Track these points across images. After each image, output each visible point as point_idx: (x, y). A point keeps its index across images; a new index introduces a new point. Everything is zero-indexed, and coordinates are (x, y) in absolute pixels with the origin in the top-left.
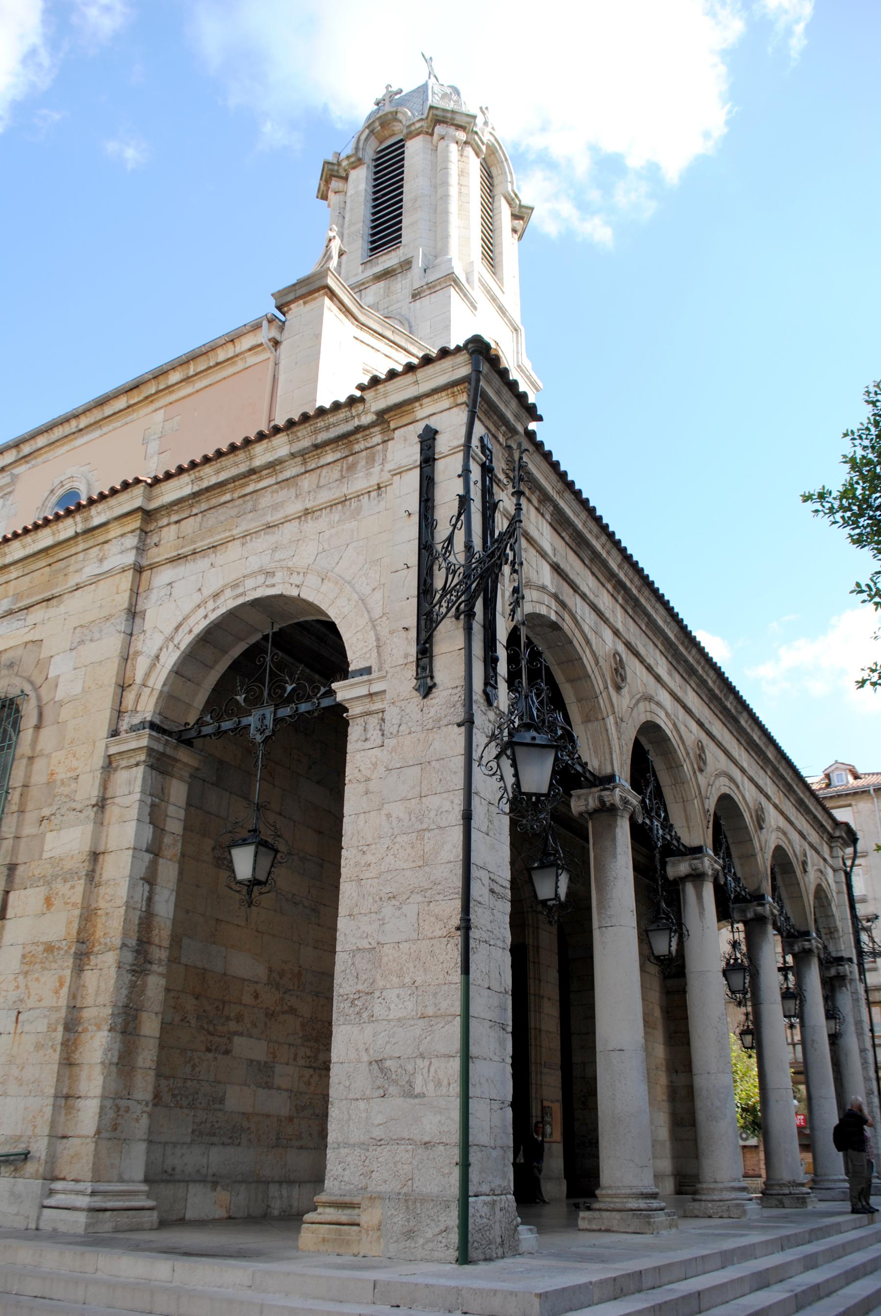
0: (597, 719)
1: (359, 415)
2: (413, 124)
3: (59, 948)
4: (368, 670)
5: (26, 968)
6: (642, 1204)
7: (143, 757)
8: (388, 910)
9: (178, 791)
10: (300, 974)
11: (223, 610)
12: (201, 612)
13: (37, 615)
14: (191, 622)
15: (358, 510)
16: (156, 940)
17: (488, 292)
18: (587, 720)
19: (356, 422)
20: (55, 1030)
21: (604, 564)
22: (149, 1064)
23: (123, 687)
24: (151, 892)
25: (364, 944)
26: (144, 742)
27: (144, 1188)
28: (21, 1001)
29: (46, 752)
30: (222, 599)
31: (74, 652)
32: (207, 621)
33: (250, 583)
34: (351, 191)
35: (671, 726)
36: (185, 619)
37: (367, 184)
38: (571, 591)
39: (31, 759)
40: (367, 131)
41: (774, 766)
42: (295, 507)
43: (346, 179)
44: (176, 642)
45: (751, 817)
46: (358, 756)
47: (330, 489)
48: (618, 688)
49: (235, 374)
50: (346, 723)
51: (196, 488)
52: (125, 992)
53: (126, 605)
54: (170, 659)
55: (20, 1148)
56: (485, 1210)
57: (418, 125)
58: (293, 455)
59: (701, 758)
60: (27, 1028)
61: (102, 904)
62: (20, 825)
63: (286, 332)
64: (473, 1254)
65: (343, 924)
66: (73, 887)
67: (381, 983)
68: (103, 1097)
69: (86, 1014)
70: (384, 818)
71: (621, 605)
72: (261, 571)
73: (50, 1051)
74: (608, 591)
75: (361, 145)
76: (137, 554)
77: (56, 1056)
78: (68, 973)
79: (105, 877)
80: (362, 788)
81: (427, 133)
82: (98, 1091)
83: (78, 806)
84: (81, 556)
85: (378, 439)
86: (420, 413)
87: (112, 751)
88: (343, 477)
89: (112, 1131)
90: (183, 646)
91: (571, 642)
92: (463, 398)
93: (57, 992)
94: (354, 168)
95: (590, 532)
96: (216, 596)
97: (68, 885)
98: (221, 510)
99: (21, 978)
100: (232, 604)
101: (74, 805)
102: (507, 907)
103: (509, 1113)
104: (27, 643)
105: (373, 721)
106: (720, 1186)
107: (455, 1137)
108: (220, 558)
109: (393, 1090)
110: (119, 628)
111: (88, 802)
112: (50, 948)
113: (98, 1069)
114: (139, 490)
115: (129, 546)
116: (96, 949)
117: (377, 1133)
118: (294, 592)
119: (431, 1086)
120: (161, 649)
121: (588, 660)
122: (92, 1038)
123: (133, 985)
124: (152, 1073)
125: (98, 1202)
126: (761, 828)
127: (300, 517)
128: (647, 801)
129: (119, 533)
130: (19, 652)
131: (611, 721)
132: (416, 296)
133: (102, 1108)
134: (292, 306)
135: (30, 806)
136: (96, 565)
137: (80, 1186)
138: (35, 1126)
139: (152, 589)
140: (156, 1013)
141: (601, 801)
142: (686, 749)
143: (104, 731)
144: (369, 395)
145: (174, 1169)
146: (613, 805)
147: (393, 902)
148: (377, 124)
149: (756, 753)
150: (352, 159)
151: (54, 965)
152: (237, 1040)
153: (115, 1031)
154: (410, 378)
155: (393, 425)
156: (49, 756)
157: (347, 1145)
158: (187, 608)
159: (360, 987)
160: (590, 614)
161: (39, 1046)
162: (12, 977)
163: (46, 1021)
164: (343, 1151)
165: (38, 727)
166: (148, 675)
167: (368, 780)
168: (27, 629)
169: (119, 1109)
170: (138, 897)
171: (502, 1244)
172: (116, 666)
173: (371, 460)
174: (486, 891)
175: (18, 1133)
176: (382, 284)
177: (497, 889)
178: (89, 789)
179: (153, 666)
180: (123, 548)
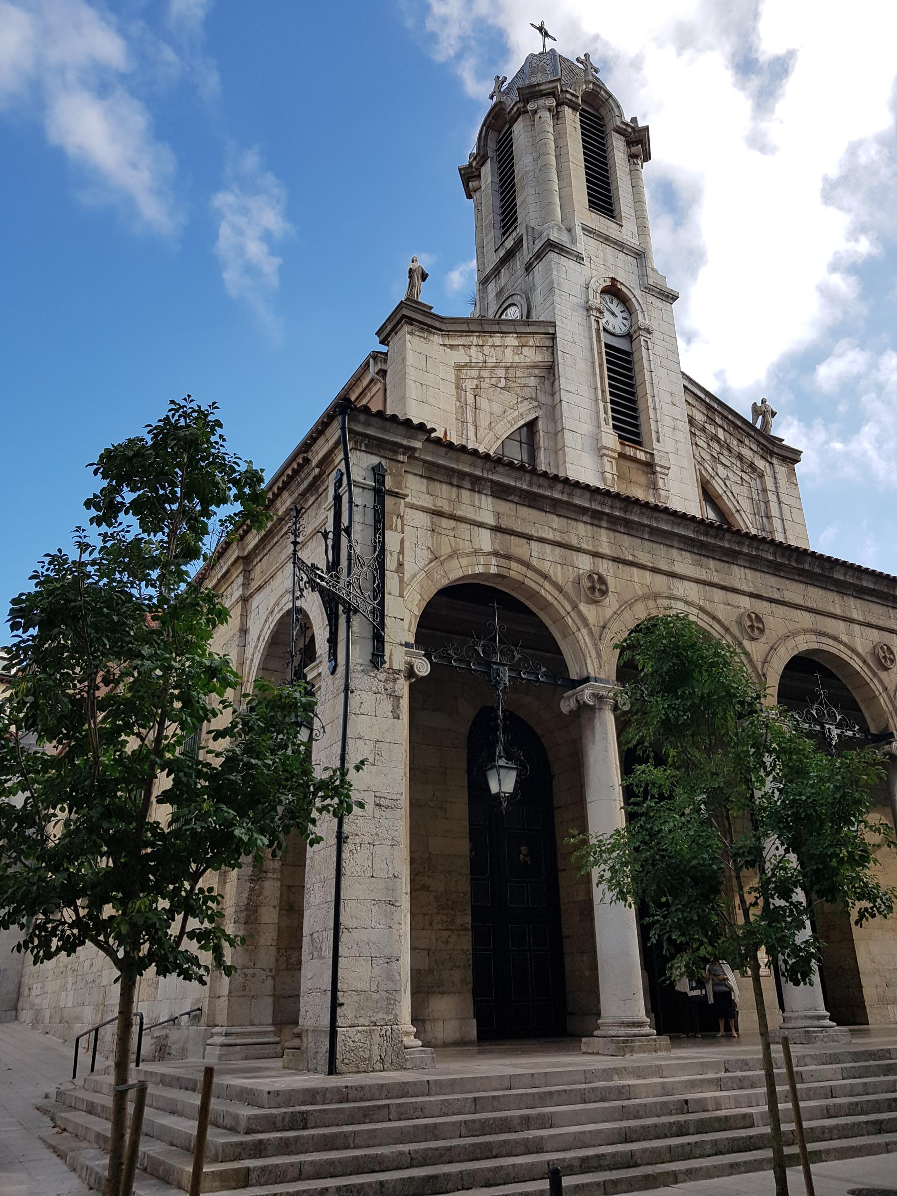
10: (430, 859)
18: (564, 637)
22: (270, 942)
27: (271, 1028)
45: (865, 662)
52: (246, 895)
71: (607, 528)
74: (585, 523)
95: (540, 486)
96: (272, 612)
114: (234, 545)
123: (252, 890)
124: (274, 949)
140: (274, 907)
149: (877, 597)
153: (239, 923)
179: (251, 666)
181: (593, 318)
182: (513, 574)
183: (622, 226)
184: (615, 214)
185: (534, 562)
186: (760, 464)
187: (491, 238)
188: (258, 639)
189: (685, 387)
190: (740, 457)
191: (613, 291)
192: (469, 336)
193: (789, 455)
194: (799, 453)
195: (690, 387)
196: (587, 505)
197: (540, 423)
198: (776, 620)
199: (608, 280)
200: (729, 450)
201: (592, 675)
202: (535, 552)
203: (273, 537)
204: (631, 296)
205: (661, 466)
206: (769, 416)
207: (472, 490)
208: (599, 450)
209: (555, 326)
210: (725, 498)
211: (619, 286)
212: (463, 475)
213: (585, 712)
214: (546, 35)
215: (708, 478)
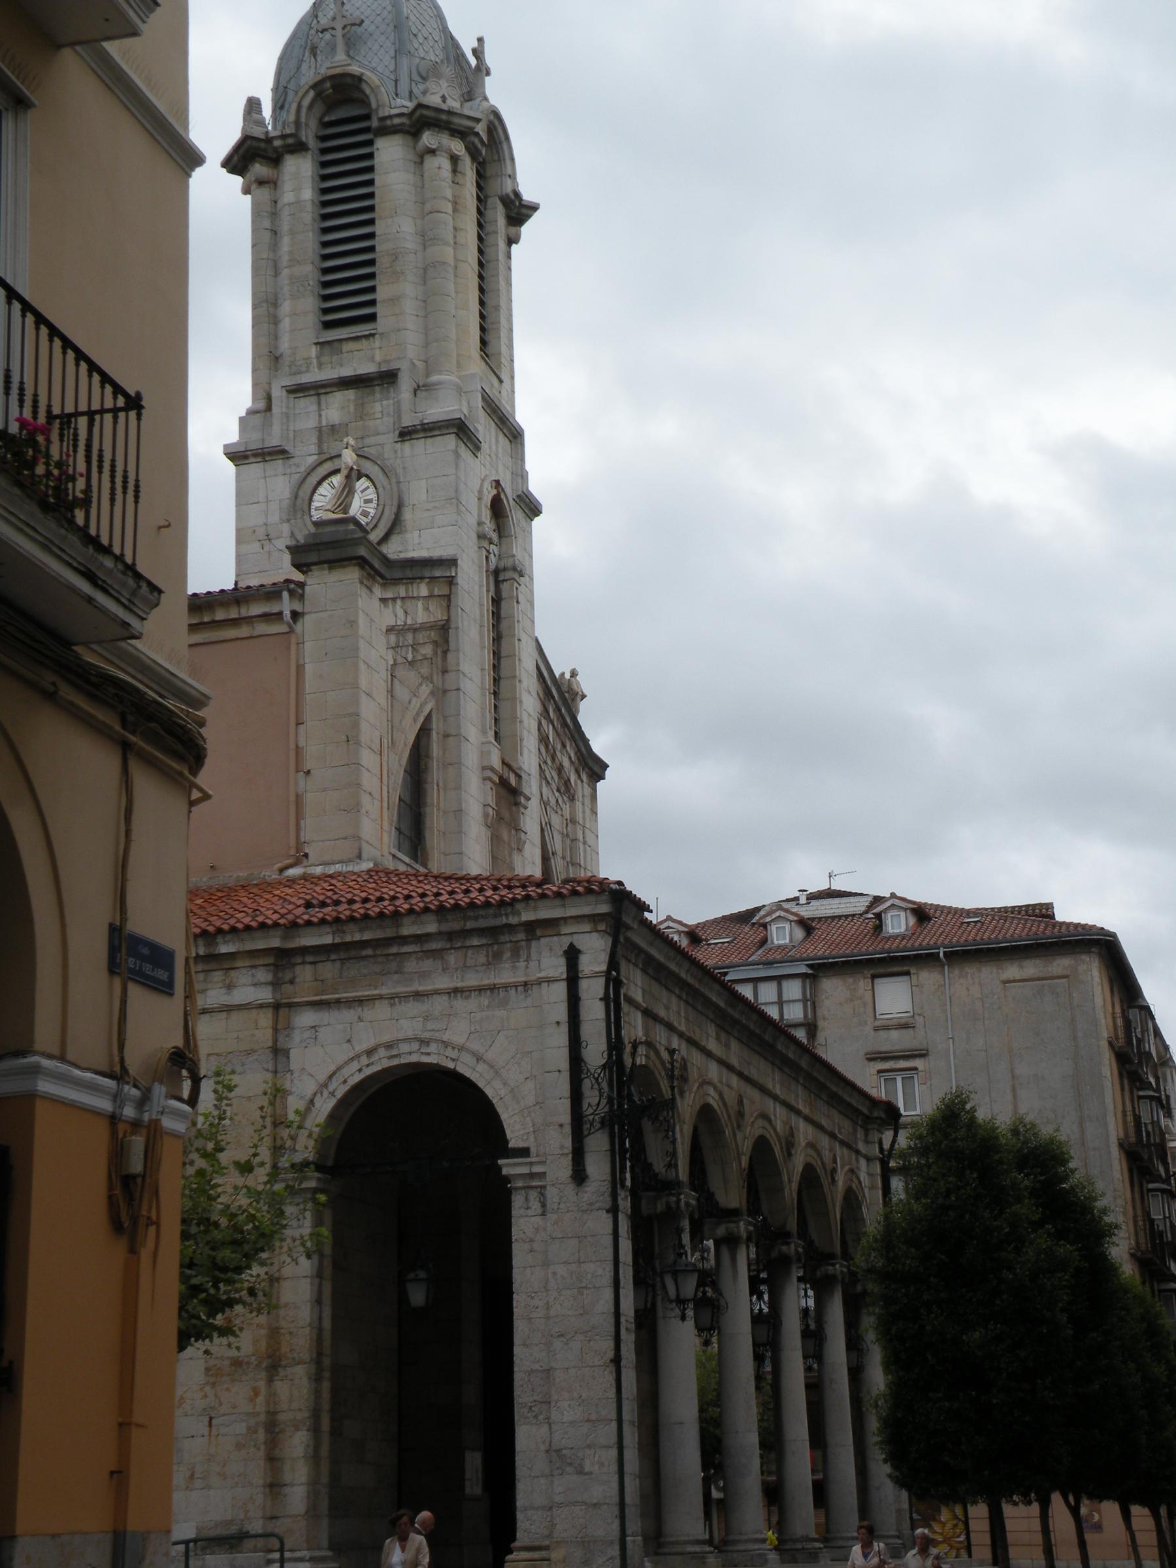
2: (391, 117)
3: (248, 1363)
4: (524, 1152)
5: (212, 1380)
6: (697, 1548)
8: (558, 1344)
12: (355, 1066)
14: (346, 1072)
19: (504, 920)
20: (256, 1432)
25: (537, 1367)
27: (330, 1553)
28: (212, 1408)
30: (375, 1057)
33: (404, 1047)
35: (717, 1097)
36: (339, 1069)
44: (331, 1089)
46: (522, 1221)
51: (338, 940)
53: (270, 1044)
54: (325, 1106)
58: (440, 933)
61: (283, 1324)
63: (306, 602)
65: (518, 1350)
67: (555, 1397)
69: (281, 1417)
72: (416, 1039)
73: (252, 1449)
75: (303, 120)
76: (274, 991)
77: (261, 1453)
78: (262, 1384)
79: (283, 1300)
80: (527, 1246)
81: (408, 133)
82: (304, 1479)
86: (565, 930)
93: (251, 1400)
96: (370, 1052)
99: (208, 1389)
100: (386, 1064)
105: (533, 1195)
106: (745, 1537)
107: (616, 1499)
108: (368, 1013)
109: (568, 1469)
110: (266, 1066)
115: (263, 980)
116: (283, 1363)
117: (558, 1499)
118: (451, 1065)
119: (596, 1467)
120: (315, 1094)
129: (247, 964)
134: (313, 567)
136: (223, 991)
137: (298, 1554)
139: (293, 1028)
148: (328, 85)
150: (290, 141)
154: (558, 902)
157: (532, 1508)
159: (535, 1398)
161: (239, 1446)
163: (244, 1424)
164: (530, 1513)
173: (516, 954)
175: (229, 1518)
176: (351, 394)
180: (255, 981)
183: (501, 381)
186: (573, 778)
188: (331, 1077)
193: (596, 768)
208: (484, 768)
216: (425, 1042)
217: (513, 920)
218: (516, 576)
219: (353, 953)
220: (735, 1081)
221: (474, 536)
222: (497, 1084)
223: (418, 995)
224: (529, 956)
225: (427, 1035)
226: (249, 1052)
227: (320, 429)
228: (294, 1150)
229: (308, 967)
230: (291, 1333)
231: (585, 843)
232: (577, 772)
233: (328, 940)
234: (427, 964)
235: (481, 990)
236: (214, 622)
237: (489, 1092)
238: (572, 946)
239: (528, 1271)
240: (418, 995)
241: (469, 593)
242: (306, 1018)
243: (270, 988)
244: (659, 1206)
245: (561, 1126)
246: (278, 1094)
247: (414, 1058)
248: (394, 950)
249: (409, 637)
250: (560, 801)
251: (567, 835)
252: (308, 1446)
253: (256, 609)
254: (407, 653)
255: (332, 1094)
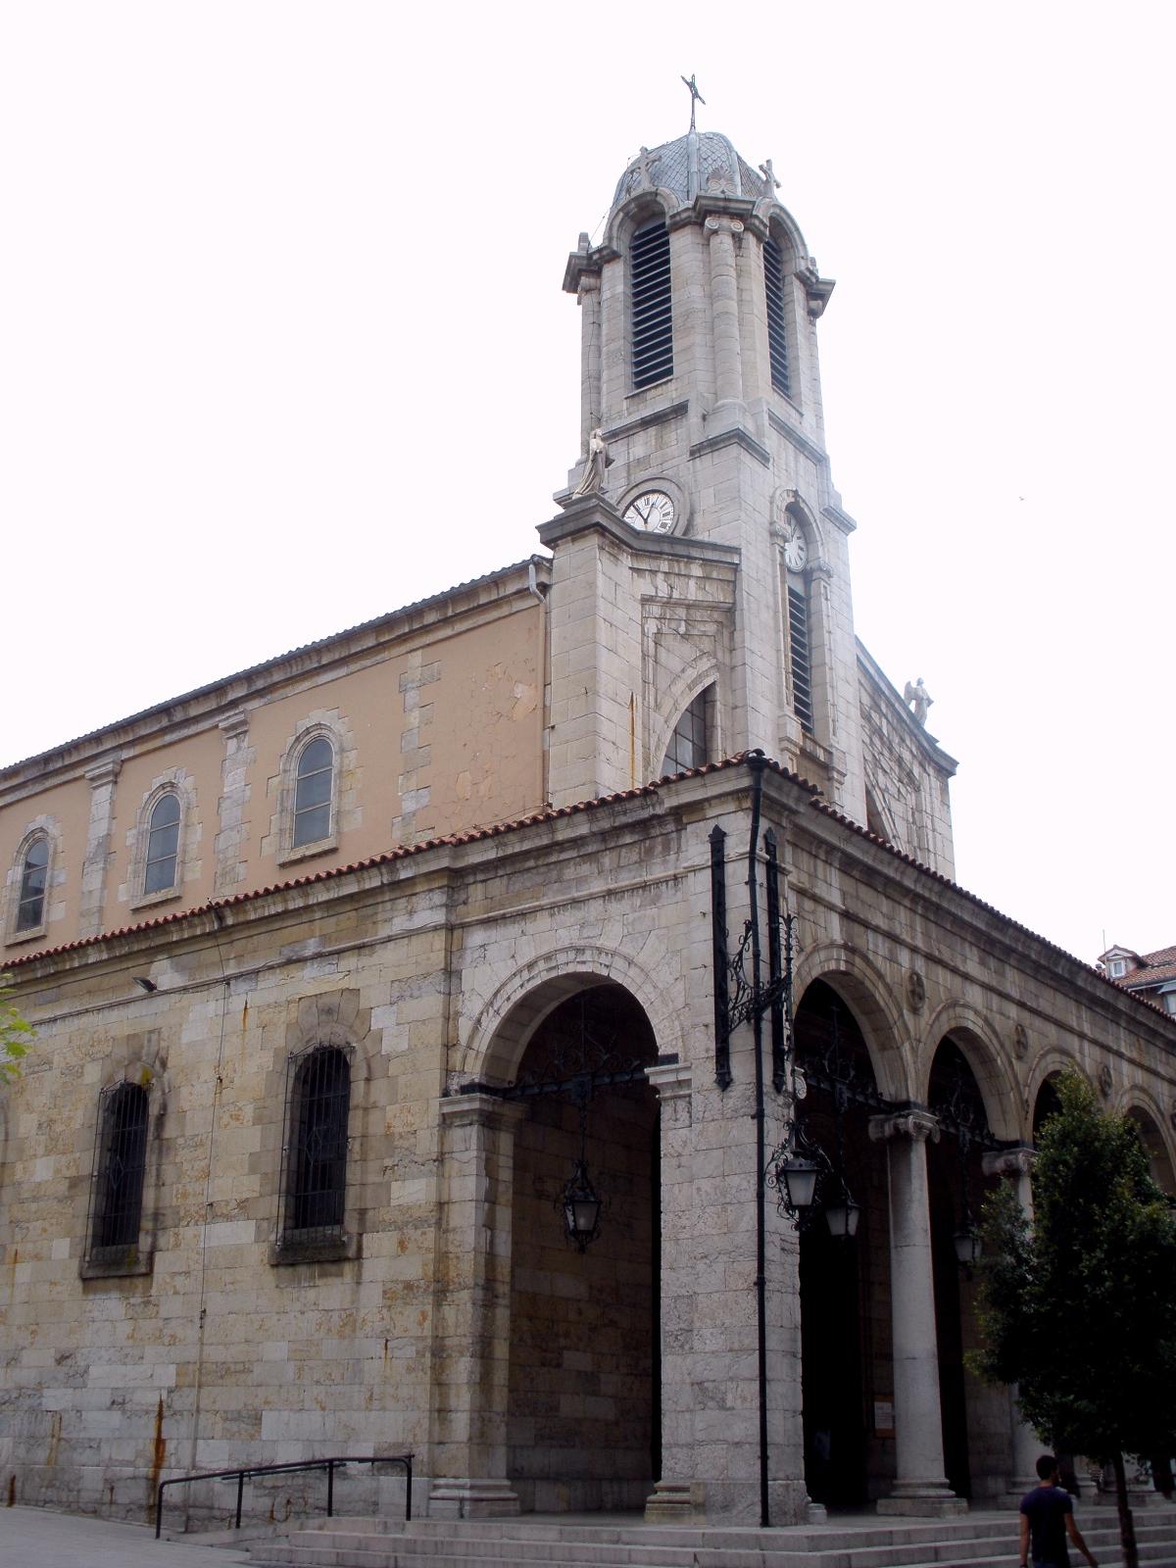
0: (892, 1047)
1: (653, 806)
2: (678, 213)
3: (418, 1287)
4: (672, 1059)
5: (389, 1302)
7: (475, 1118)
8: (701, 1266)
9: (505, 1142)
11: (538, 982)
12: (517, 981)
13: (350, 962)
14: (509, 989)
15: (658, 897)
16: (500, 1278)
17: (782, 428)
18: (883, 1048)
20: (424, 1356)
21: (899, 885)
22: (502, 1382)
23: (449, 1046)
24: (493, 1236)
26: (476, 1105)
27: (507, 1483)
28: (388, 1331)
29: (380, 1104)
30: (535, 972)
31: (395, 1007)
32: (523, 991)
33: (562, 958)
34: (606, 294)
35: (981, 1022)
36: (503, 985)
37: (625, 284)
38: (862, 929)
39: (366, 1109)
40: (621, 214)
41: (1126, 1014)
42: (598, 886)
43: (598, 273)
46: (670, 1134)
47: (630, 871)
48: (915, 1011)
49: (500, 619)
50: (658, 1104)
52: (479, 1323)
53: (442, 966)
54: (491, 1024)
55: (404, 1452)
56: (781, 1490)
57: (684, 215)
58: (594, 834)
59: (1021, 1044)
60: (397, 1353)
61: (451, 1248)
62: (364, 1172)
63: (554, 574)
64: (771, 1519)
66: (424, 1233)
67: (697, 1324)
68: (472, 1411)
69: (448, 1342)
70: (695, 1192)
73: (421, 1373)
77: (427, 1379)
78: (429, 1308)
79: (451, 1225)
80: (674, 1162)
81: (695, 223)
82: (467, 1406)
83: (420, 1160)
84: (388, 905)
85: (671, 827)
86: (710, 813)
87: (447, 1109)
88: (641, 861)
89: (481, 1439)
90: (503, 1013)
91: (863, 983)
92: (748, 804)
93: (421, 1324)
94: (608, 261)
96: (530, 966)
97: (419, 1232)
98: (527, 876)
99: (385, 1311)
100: (546, 976)
101: (416, 1159)
102: (797, 1259)
103: (800, 1419)
104: (343, 991)
105: (682, 1104)
107: (758, 1438)
108: (530, 926)
109: (711, 1404)
111: (429, 1157)
112: (409, 1286)
113: (465, 1389)
114: (446, 851)
116: (451, 1288)
117: (699, 1436)
118: (605, 973)
119: (739, 1401)
120: (482, 1013)
121: (880, 995)
122: (456, 1362)
123: (485, 1317)
124: (506, 1390)
125: (477, 1494)
126: (1105, 1094)
127: (604, 896)
128: (952, 1109)
129: (426, 888)
130: (336, 999)
131: (906, 1048)
132: (696, 452)
133: (472, 1419)
135: (372, 1156)
136: (406, 917)
137: (461, 1481)
138: (415, 1435)
141: (896, 1128)
142: (999, 1041)
143: (436, 1092)
144: (661, 792)
145: (522, 1468)
146: (907, 1133)
147: (705, 1260)
151: (415, 1302)
152: (566, 1354)
154: (698, 781)
155: (685, 820)
156: (384, 1108)
157: (677, 1445)
158: (505, 975)
159: (682, 1326)
160: (884, 942)
161: (410, 1370)
162: (376, 1310)
164: (674, 1450)
165: (368, 1080)
166: (472, 1038)
167: (680, 1155)
168: (341, 975)
169: (483, 1420)
170: (482, 1242)
171: (795, 1515)
172: (440, 1027)
173: (666, 849)
174: (778, 1251)
175: (400, 1440)
176: (652, 431)
177: (787, 1246)
178: (427, 1143)
181: (778, 548)
182: (856, 972)
183: (802, 415)
184: (792, 392)
185: (871, 956)
186: (916, 771)
187: (619, 373)
188: (495, 995)
189: (858, 659)
190: (900, 761)
191: (795, 511)
192: (657, 558)
193: (944, 763)
194: (955, 763)
195: (862, 658)
196: (913, 887)
197: (718, 689)
198: (1042, 1035)
199: (791, 494)
200: (891, 750)
201: (912, 1099)
202: (876, 946)
203: (528, 859)
204: (812, 520)
205: (838, 772)
206: (925, 704)
207: (826, 862)
208: (781, 740)
209: (740, 554)
210: (884, 818)
211: (802, 505)
212: (821, 842)
213: (902, 1141)
214: (695, 95)
215: (870, 788)
216: (580, 950)
217: (659, 811)
218: (824, 577)
219: (518, 866)
220: (1013, 1011)
221: (766, 535)
222: (648, 988)
223: (576, 902)
224: (679, 848)
225: (582, 943)
226: (425, 976)
227: (628, 465)
228: (463, 1072)
229: (479, 885)
230: (458, 1258)
231: (934, 830)
232: (921, 765)
233: (492, 855)
234: (585, 869)
235: (633, 889)
236: (479, 606)
237: (640, 997)
238: (717, 829)
239: (676, 1189)
240: (576, 902)
241: (758, 581)
242: (477, 937)
243: (444, 909)
244: (887, 1128)
245: (706, 1026)
246: (449, 1017)
247: (571, 969)
248: (553, 859)
249: (682, 612)
250: (903, 790)
251: (914, 823)
252: (472, 1372)
253: (511, 588)
254: (680, 626)
255: (497, 1012)
